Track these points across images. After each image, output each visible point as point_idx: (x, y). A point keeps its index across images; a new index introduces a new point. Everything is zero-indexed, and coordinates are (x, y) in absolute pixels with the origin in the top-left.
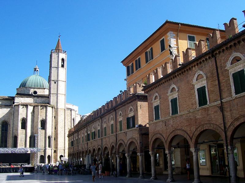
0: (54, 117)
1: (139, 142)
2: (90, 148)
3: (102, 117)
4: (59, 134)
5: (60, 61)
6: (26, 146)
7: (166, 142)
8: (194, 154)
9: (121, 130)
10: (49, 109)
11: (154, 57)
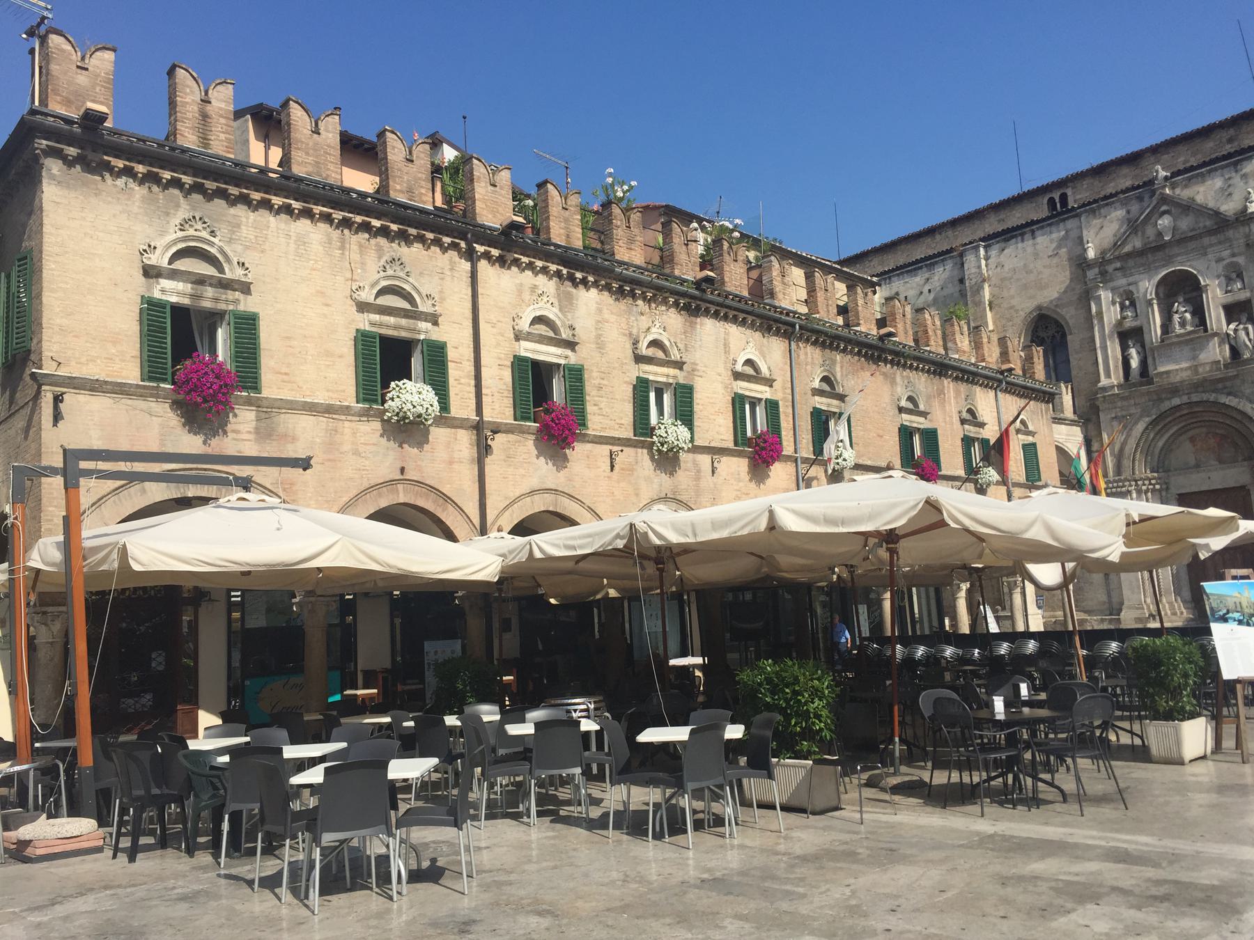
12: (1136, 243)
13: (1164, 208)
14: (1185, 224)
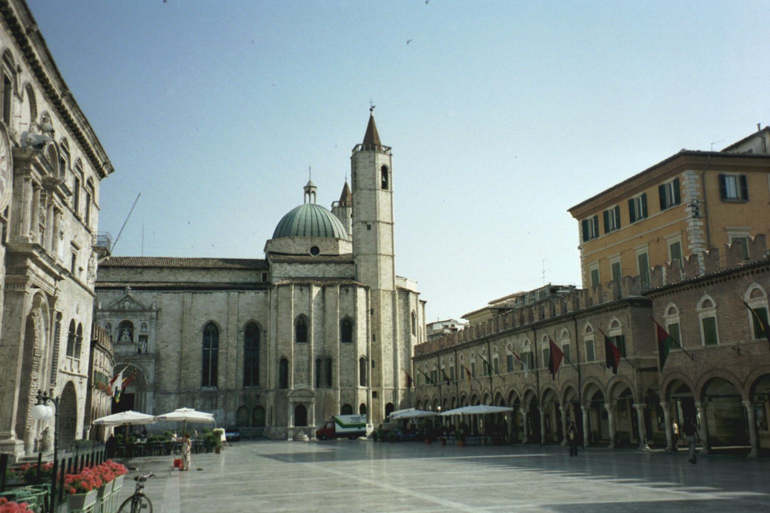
0: (370, 312)
1: (635, 383)
2: (498, 390)
3: (535, 327)
4: (383, 352)
5: (379, 173)
6: (309, 383)
7: (695, 387)
8: (748, 410)
9: (591, 357)
10: (361, 292)
11: (649, 212)
12: (116, 307)
13: (127, 299)
14: (133, 306)
